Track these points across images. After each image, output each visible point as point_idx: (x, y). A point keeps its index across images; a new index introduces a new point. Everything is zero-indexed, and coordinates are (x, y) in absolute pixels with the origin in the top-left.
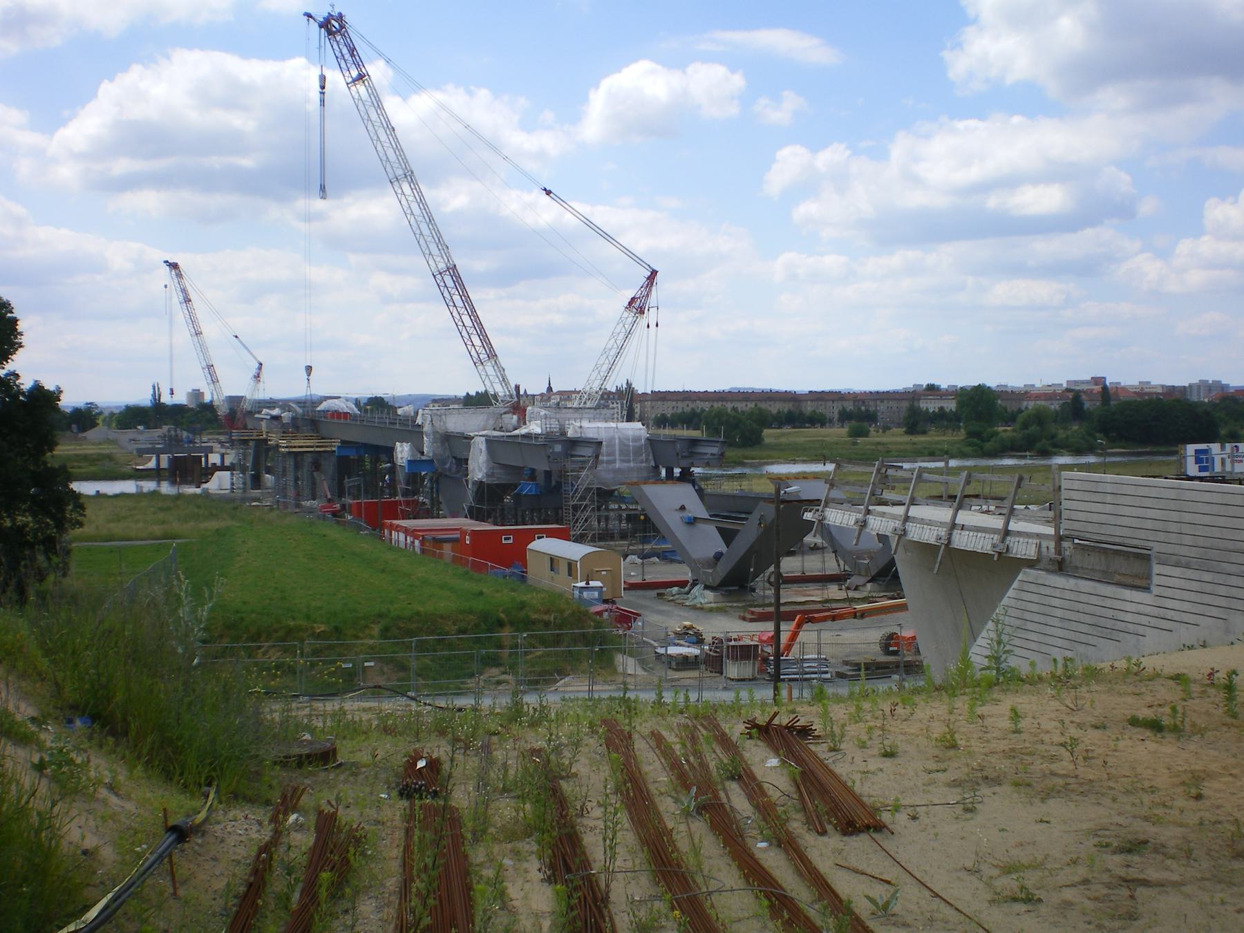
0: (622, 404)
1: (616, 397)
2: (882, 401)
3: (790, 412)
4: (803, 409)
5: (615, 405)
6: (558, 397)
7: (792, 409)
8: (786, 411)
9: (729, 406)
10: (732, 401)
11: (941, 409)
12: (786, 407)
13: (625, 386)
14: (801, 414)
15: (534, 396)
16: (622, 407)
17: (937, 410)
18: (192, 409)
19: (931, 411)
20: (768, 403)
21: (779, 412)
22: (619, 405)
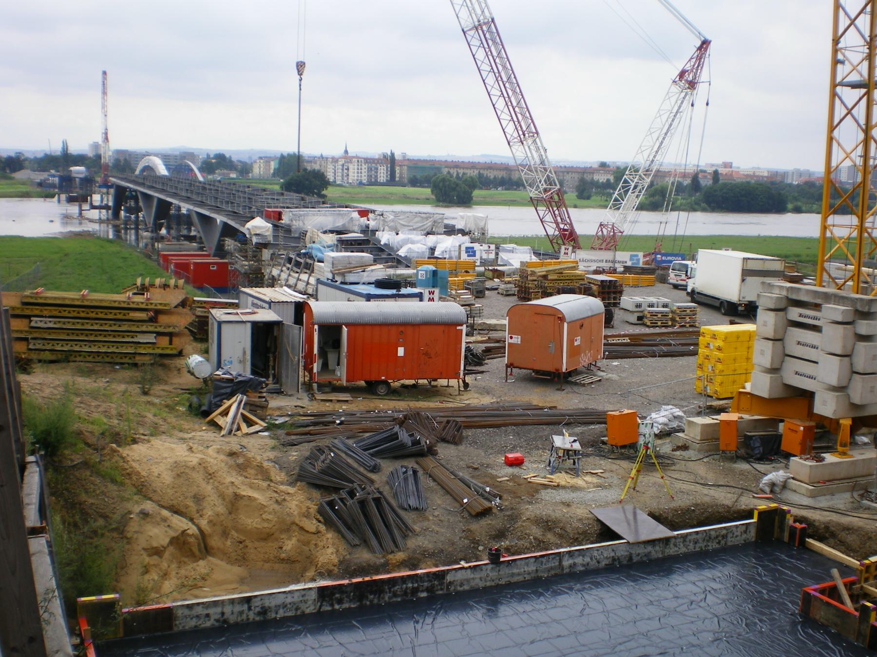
0: (387, 167)
2: (568, 173)
3: (502, 178)
4: (512, 177)
5: (382, 167)
6: (343, 160)
7: (505, 176)
8: (500, 177)
9: (461, 171)
10: (463, 168)
11: (608, 180)
12: (500, 174)
13: (389, 154)
14: (510, 179)
15: (327, 158)
16: (387, 169)
17: (605, 181)
18: (90, 158)
19: (601, 181)
20: (489, 171)
21: (495, 177)
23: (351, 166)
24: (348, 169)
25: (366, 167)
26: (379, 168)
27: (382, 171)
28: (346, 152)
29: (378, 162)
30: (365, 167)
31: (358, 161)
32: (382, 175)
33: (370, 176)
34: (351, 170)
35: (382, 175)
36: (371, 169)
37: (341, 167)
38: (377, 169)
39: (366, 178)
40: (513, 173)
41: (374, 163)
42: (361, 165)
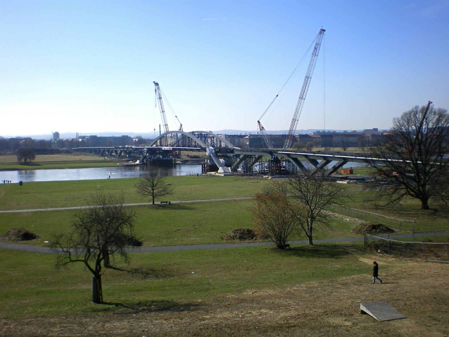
1: (237, 136)
22: (238, 140)
26: (236, 140)
29: (235, 137)
36: (232, 141)
38: (234, 140)
41: (233, 137)
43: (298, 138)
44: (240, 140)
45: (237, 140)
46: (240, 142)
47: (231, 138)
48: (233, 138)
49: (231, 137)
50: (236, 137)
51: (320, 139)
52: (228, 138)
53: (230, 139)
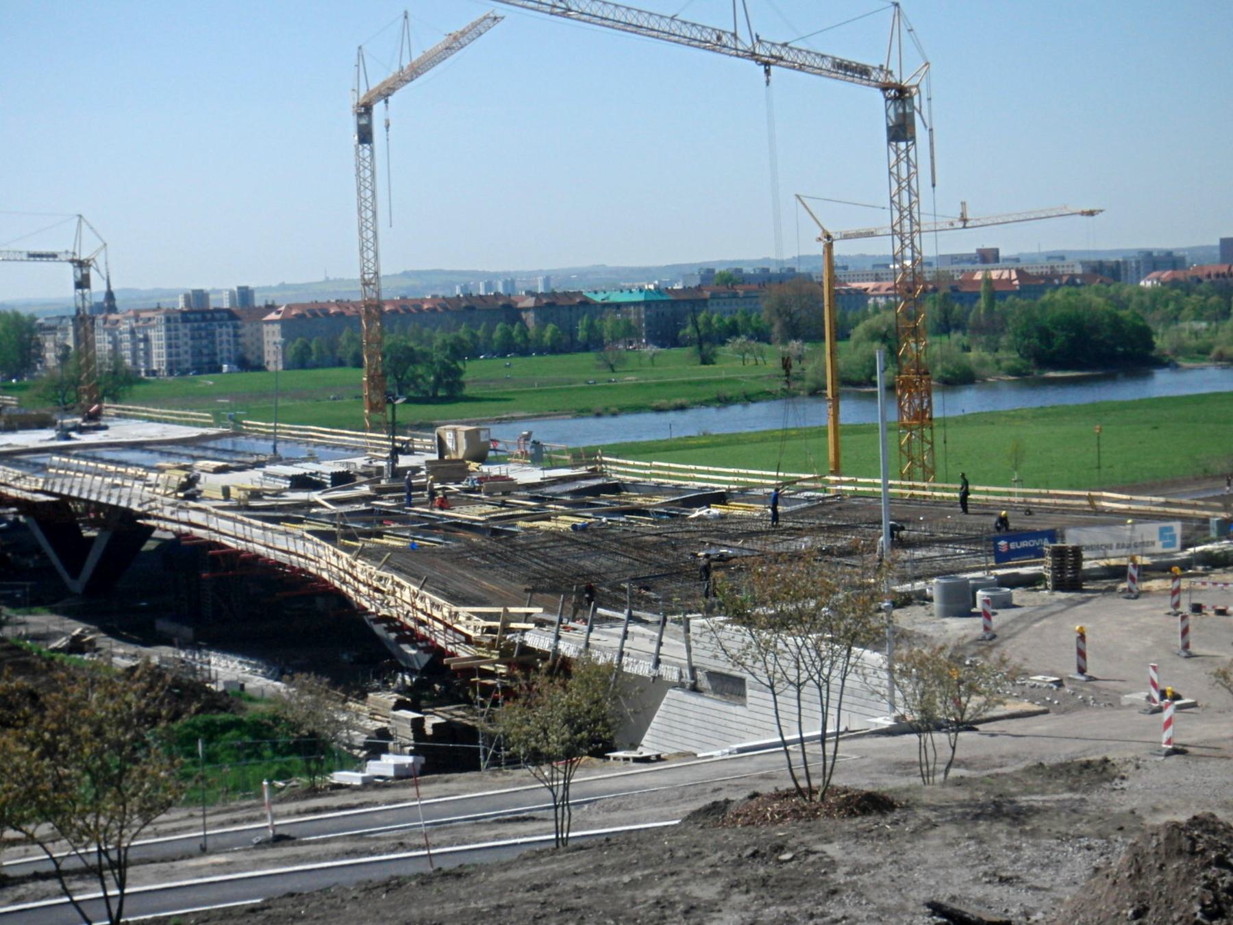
1: (226, 315)
22: (231, 330)
23: (152, 334)
24: (146, 340)
25: (187, 331)
26: (218, 331)
27: (225, 338)
28: (110, 295)
29: (213, 319)
30: (184, 330)
31: (168, 320)
32: (225, 346)
33: (197, 353)
34: (154, 342)
35: (225, 346)
37: (127, 336)
38: (213, 334)
39: (188, 357)
40: (524, 315)
41: (204, 319)
42: (176, 329)
43: (527, 309)
44: (240, 332)
45: (224, 329)
46: (241, 340)
47: (196, 325)
48: (203, 324)
49: (196, 320)
50: (222, 319)
51: (642, 309)
52: (180, 326)
53: (192, 330)
